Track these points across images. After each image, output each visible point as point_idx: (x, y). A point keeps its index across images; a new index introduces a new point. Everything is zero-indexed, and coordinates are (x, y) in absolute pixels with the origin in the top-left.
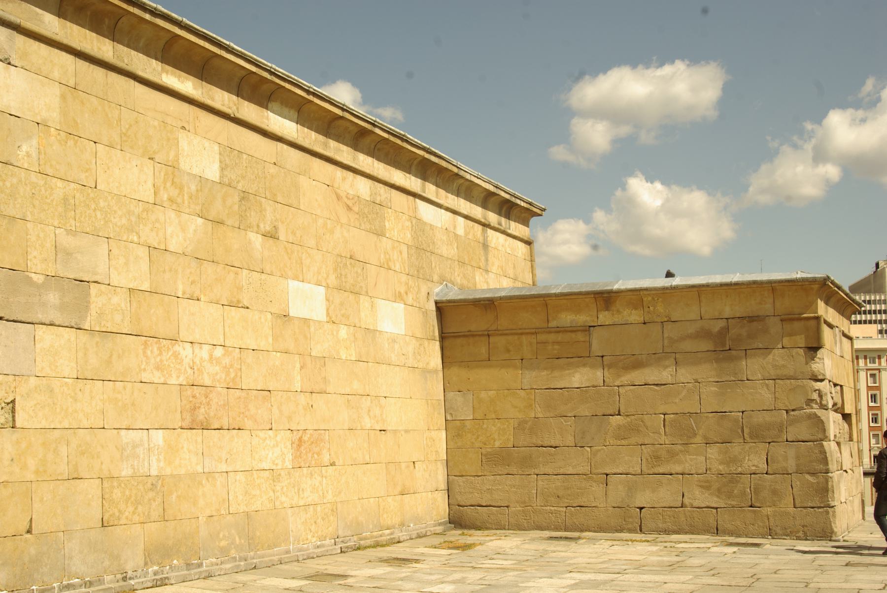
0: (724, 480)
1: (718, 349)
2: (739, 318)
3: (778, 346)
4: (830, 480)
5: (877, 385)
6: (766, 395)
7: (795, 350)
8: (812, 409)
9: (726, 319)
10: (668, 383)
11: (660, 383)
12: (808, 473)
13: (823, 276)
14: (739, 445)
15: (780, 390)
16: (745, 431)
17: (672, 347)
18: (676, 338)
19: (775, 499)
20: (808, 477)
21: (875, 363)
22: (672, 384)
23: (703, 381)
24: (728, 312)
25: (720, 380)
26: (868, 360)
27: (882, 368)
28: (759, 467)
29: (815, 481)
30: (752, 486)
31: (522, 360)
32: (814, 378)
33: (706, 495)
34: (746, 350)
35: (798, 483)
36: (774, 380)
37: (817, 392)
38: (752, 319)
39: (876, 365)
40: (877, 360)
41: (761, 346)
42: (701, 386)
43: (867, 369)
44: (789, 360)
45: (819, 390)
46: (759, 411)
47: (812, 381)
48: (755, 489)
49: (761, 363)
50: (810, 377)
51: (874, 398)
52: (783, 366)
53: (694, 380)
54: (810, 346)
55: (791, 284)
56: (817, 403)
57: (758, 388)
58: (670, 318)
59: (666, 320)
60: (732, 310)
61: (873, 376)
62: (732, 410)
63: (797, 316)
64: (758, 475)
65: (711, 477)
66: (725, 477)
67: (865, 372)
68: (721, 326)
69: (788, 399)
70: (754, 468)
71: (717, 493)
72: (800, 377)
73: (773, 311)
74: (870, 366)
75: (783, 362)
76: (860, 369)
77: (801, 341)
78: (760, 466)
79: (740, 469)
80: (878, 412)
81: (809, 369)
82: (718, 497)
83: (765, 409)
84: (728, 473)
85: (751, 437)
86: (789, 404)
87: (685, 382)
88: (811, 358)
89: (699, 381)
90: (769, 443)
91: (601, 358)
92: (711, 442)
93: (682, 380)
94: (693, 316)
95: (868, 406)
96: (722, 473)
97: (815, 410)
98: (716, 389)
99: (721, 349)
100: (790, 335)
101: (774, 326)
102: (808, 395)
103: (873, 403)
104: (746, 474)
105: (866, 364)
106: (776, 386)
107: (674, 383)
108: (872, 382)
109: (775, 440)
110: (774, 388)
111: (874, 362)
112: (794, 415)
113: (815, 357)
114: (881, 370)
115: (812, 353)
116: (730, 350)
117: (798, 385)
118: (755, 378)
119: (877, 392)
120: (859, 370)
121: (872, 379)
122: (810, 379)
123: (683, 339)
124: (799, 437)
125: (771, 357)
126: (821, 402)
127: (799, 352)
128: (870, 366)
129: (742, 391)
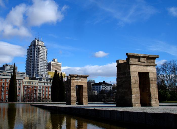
39: (20, 83)
51: (19, 89)
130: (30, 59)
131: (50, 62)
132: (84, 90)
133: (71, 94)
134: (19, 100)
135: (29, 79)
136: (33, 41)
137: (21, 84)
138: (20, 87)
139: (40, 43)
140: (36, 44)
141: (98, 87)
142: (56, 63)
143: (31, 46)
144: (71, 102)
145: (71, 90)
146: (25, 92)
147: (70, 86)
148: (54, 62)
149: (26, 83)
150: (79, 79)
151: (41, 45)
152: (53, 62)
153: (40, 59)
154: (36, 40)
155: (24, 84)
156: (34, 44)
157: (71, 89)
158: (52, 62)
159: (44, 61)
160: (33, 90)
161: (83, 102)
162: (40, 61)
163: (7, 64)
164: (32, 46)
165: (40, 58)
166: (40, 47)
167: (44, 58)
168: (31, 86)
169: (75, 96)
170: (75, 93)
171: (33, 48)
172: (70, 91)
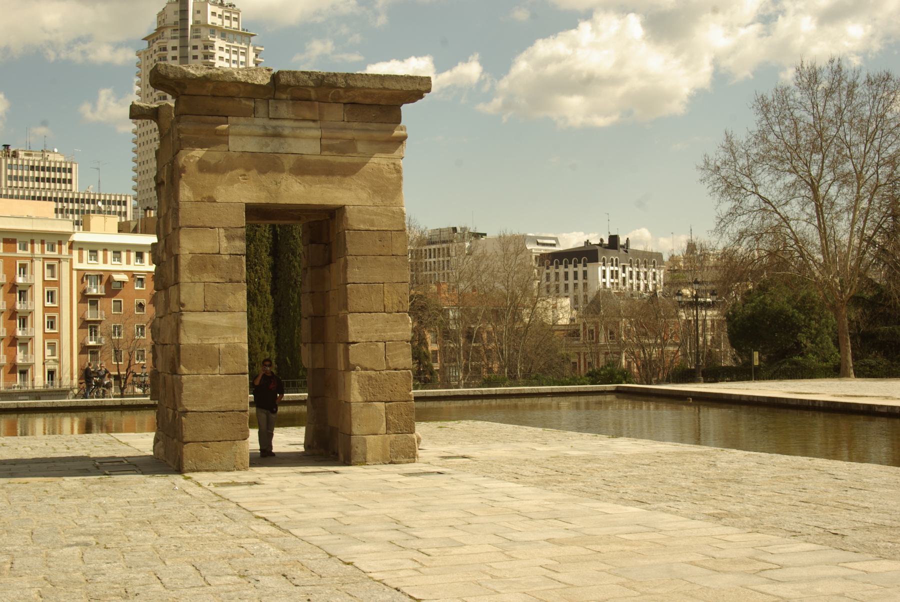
5: (55, 279)
21: (55, 251)
26: (46, 245)
27: (63, 257)
39: (55, 254)
40: (57, 246)
43: (43, 258)
51: (51, 294)
61: (51, 267)
67: (41, 262)
74: (48, 253)
76: (34, 257)
80: (56, 315)
95: (44, 307)
103: (50, 303)
105: (43, 251)
108: (50, 275)
111: (53, 250)
114: (62, 260)
119: (56, 289)
120: (34, 259)
121: (50, 271)
128: (48, 253)
132: (355, 274)
133: (179, 323)
134: (57, 367)
135: (119, 231)
137: (65, 266)
138: (57, 283)
139: (214, 14)
140: (190, 22)
141: (576, 273)
144: (188, 434)
145: (185, 276)
146: (89, 318)
147: (170, 230)
149: (96, 259)
150: (287, 126)
151: (218, 22)
155: (88, 264)
156: (177, 18)
157: (183, 262)
160: (144, 301)
161: (355, 430)
163: (12, 149)
164: (168, 33)
166: (219, 42)
168: (132, 274)
169: (232, 349)
170: (242, 319)
171: (176, 43)
172: (172, 290)
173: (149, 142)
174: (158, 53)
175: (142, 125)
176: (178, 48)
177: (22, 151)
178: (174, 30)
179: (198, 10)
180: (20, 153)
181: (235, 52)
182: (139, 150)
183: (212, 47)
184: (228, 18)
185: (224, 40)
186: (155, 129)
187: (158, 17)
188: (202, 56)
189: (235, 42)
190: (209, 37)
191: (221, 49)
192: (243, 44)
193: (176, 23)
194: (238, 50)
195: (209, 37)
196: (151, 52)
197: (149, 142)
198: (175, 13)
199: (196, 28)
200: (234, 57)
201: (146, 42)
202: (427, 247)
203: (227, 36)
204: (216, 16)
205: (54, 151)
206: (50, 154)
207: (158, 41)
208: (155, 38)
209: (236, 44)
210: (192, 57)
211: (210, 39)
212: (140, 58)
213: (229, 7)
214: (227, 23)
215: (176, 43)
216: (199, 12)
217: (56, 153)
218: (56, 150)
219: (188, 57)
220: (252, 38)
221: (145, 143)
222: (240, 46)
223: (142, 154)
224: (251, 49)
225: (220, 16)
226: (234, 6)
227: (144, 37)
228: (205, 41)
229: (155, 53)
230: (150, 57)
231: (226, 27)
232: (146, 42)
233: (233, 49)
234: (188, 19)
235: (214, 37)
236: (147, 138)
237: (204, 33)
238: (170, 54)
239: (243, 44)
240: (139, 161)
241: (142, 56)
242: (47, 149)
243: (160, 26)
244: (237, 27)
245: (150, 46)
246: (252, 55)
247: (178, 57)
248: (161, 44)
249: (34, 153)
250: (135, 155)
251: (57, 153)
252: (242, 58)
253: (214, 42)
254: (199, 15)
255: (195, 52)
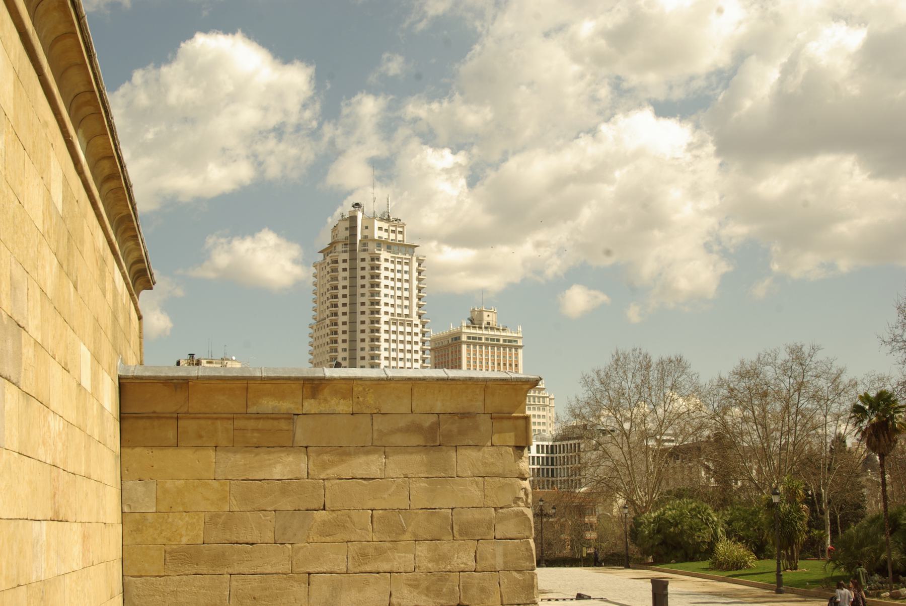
0: (433, 578)
1: (428, 445)
2: (450, 414)
3: (488, 443)
4: (535, 577)
6: (475, 493)
7: (504, 448)
8: (519, 507)
9: (437, 414)
10: (377, 477)
11: (368, 477)
12: (515, 570)
13: (535, 377)
14: (448, 543)
15: (489, 487)
16: (454, 528)
17: (381, 440)
18: (385, 431)
19: (483, 597)
20: (515, 574)
22: (381, 479)
23: (413, 476)
24: (439, 408)
25: (430, 476)
28: (468, 565)
29: (522, 578)
30: (461, 585)
31: (216, 447)
32: (521, 476)
33: (415, 594)
34: (456, 446)
35: (506, 580)
36: (484, 477)
37: (524, 490)
38: (464, 415)
41: (471, 443)
42: (411, 481)
44: (498, 458)
45: (525, 489)
46: (468, 508)
47: (519, 479)
48: (463, 587)
49: (471, 460)
50: (518, 476)
52: (493, 464)
53: (403, 475)
54: (518, 445)
55: (505, 383)
56: (523, 502)
57: (468, 484)
58: (380, 410)
59: (375, 411)
60: (443, 406)
62: (441, 507)
63: (507, 415)
64: (467, 573)
65: (420, 575)
66: (434, 576)
68: (432, 420)
69: (497, 496)
70: (463, 566)
71: (425, 592)
72: (508, 475)
73: (483, 408)
75: (492, 460)
77: (510, 438)
78: (469, 563)
79: (449, 567)
81: (517, 468)
82: (427, 596)
83: (474, 506)
84: (437, 570)
85: (460, 535)
86: (497, 502)
87: (394, 477)
88: (519, 457)
89: (409, 477)
90: (478, 540)
91: (305, 449)
92: (420, 539)
93: (392, 475)
94: (403, 409)
96: (431, 571)
97: (522, 508)
98: (426, 485)
99: (432, 445)
100: (500, 432)
101: (485, 423)
102: (516, 493)
104: (455, 572)
106: (486, 483)
107: (383, 477)
109: (484, 537)
110: (483, 485)
112: (502, 513)
113: (522, 456)
115: (520, 451)
116: (440, 446)
117: (507, 483)
118: (465, 475)
122: (517, 477)
123: (393, 432)
124: (507, 534)
125: (481, 454)
126: (527, 500)
127: (508, 451)
129: (452, 488)
130: (328, 321)
131: (453, 328)
136: (343, 219)
139: (380, 229)
140: (359, 237)
142: (490, 332)
143: (332, 244)
148: (480, 328)
151: (384, 235)
152: (472, 331)
153: (384, 318)
154: (360, 216)
156: (347, 233)
158: (465, 330)
159: (408, 329)
162: (386, 327)
163: (196, 357)
164: (340, 247)
165: (386, 313)
166: (384, 254)
167: (406, 311)
173: (323, 345)
174: (330, 265)
175: (317, 329)
176: (348, 261)
177: (205, 359)
178: (345, 244)
179: (366, 226)
180: (202, 361)
181: (399, 263)
182: (315, 353)
183: (378, 259)
184: (393, 231)
185: (390, 252)
186: (328, 333)
187: (332, 232)
188: (369, 268)
189: (400, 254)
190: (375, 250)
191: (386, 260)
192: (407, 255)
193: (346, 238)
194: (403, 261)
195: (375, 250)
196: (326, 264)
197: (323, 345)
198: (347, 229)
199: (364, 242)
200: (399, 267)
201: (322, 255)
202: (565, 443)
203: (392, 248)
204: (382, 230)
205: (232, 359)
206: (229, 363)
207: (330, 255)
208: (329, 251)
209: (400, 255)
210: (360, 269)
211: (377, 252)
212: (316, 269)
213: (395, 222)
214: (392, 236)
215: (346, 256)
216: (367, 228)
217: (234, 361)
218: (234, 358)
219: (356, 268)
220: (416, 249)
221: (320, 346)
222: (404, 257)
223: (317, 356)
224: (414, 259)
225: (386, 230)
226: (400, 220)
227: (320, 250)
228: (372, 254)
229: (328, 265)
230: (324, 268)
231: (392, 240)
232: (322, 255)
233: (397, 260)
234: (356, 235)
235: (380, 250)
236: (320, 341)
237: (371, 246)
238: (341, 266)
239: (407, 255)
240: (314, 362)
241: (318, 267)
242: (227, 357)
243: (333, 241)
244: (402, 239)
245: (325, 259)
246: (415, 265)
247: (348, 269)
248: (333, 258)
249: (215, 361)
250: (311, 357)
251: (235, 361)
252: (406, 268)
253: (380, 254)
254: (367, 230)
255: (363, 264)
